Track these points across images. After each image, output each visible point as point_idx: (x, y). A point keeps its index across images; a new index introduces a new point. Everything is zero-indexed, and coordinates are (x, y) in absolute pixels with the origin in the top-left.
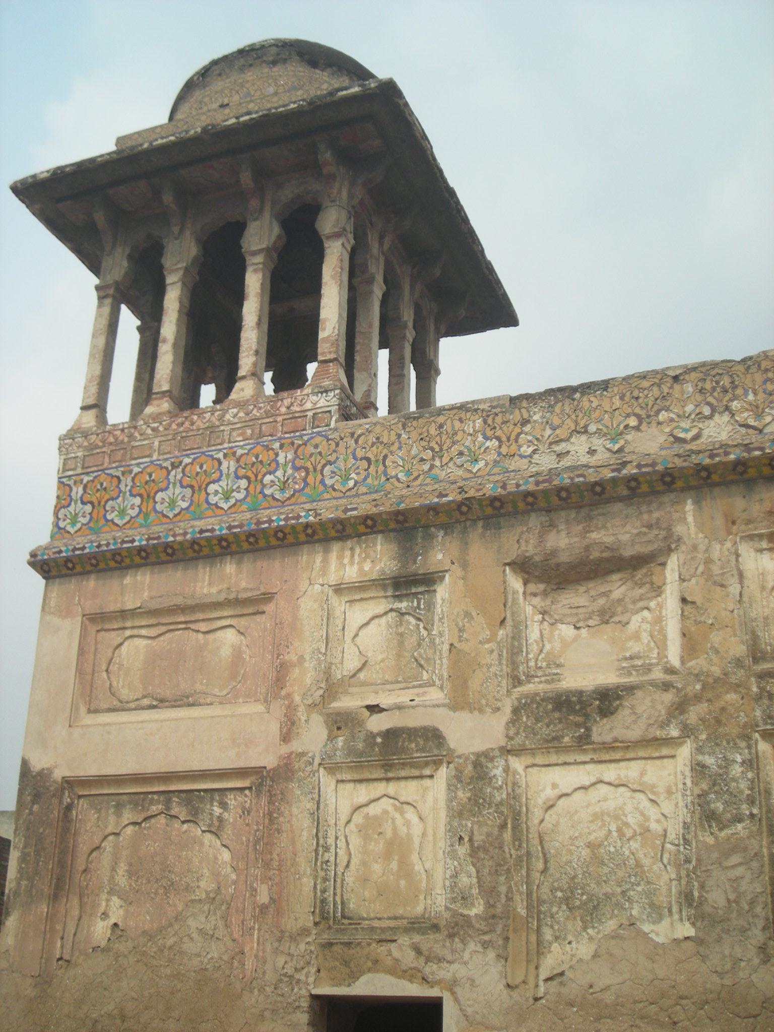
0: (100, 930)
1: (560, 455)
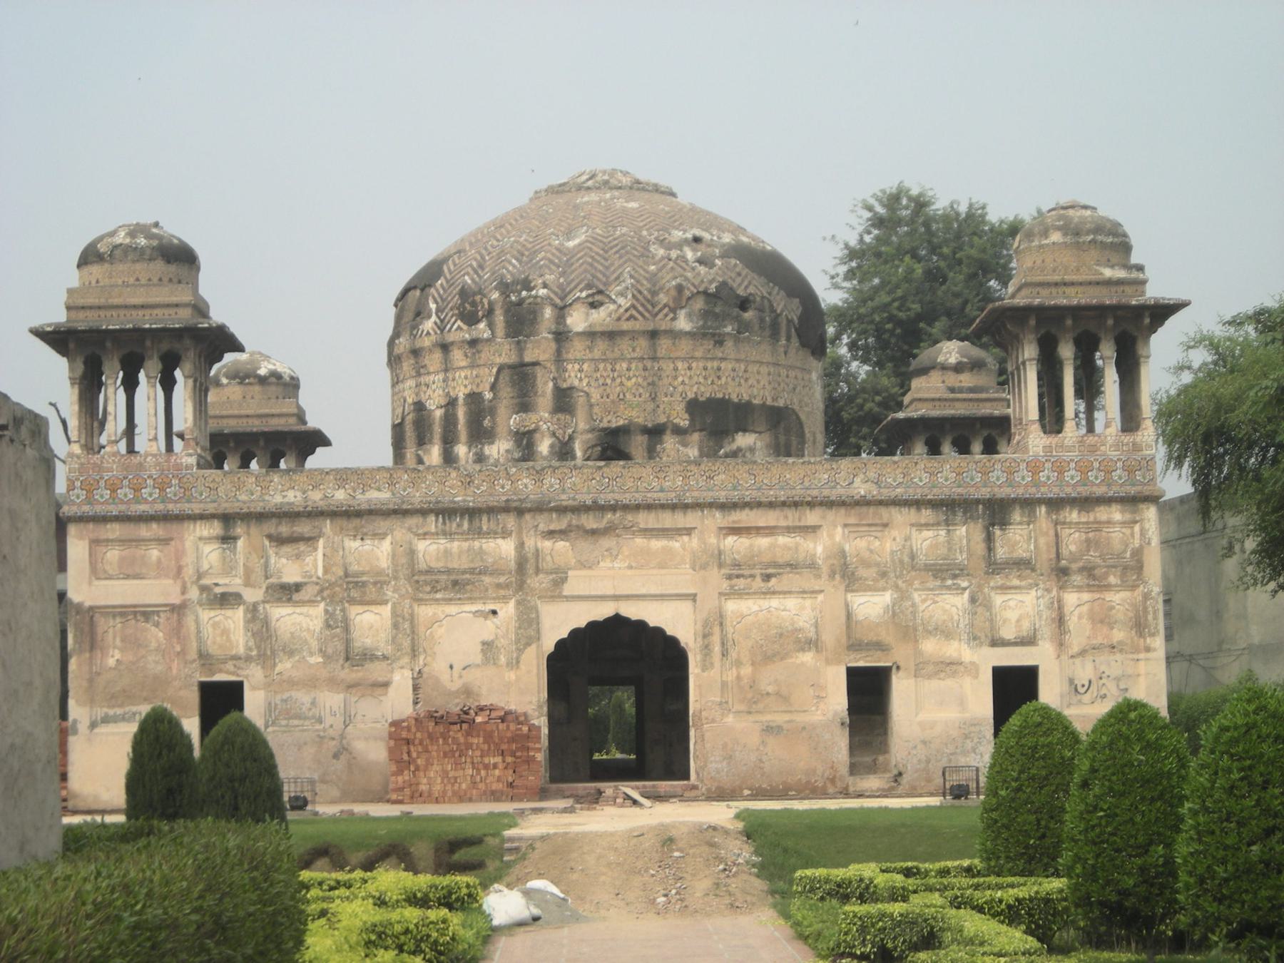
0: (111, 662)
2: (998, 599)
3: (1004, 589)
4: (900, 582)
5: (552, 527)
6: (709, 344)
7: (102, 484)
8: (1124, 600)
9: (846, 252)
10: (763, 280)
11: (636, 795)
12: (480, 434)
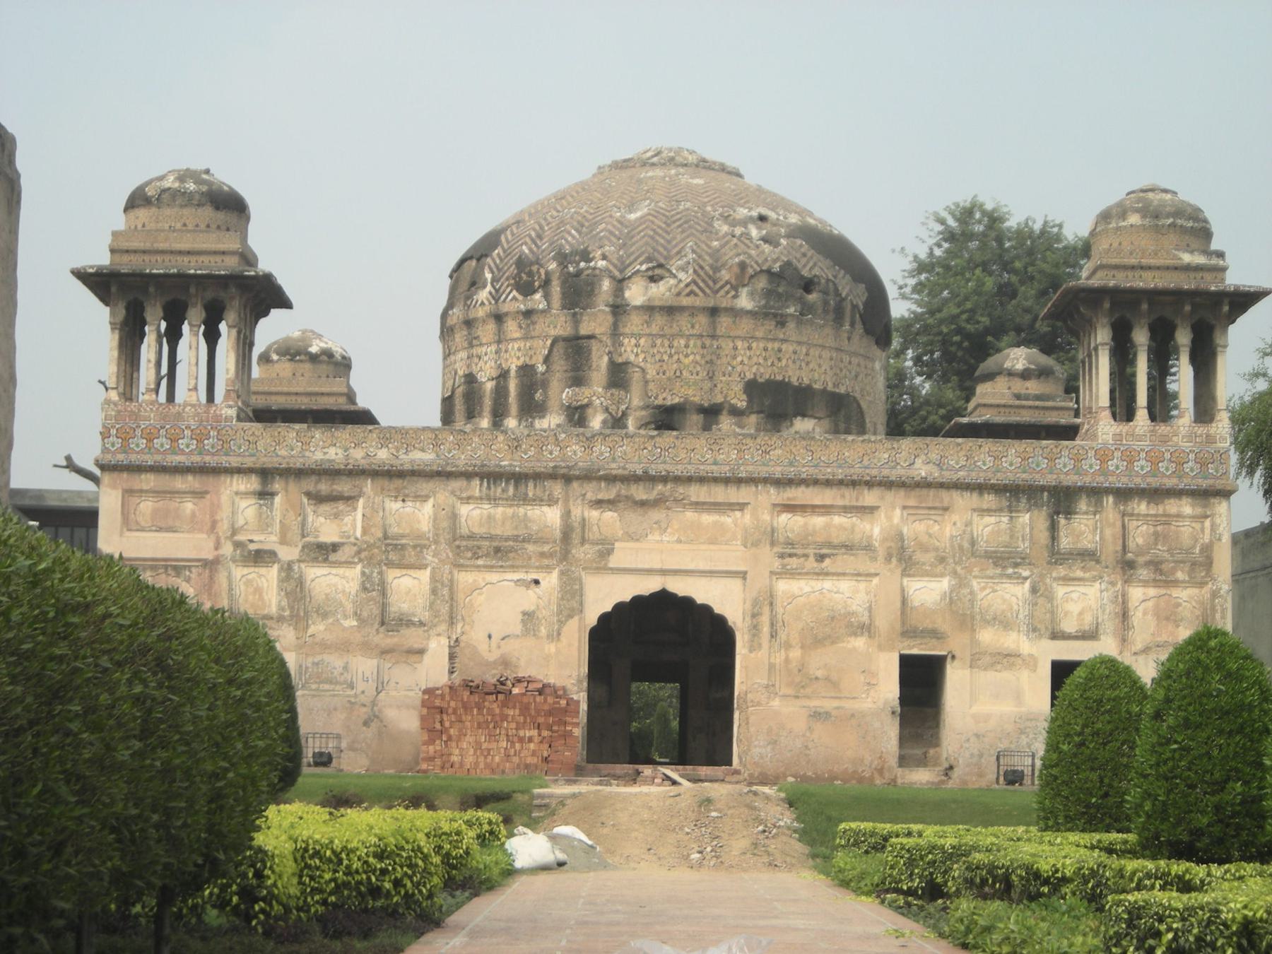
1: (325, 453)
2: (1060, 591)
3: (1067, 580)
4: (959, 569)
5: (600, 497)
6: (770, 325)
7: (139, 432)
8: (1191, 597)
9: (915, 265)
10: (829, 263)
11: (675, 776)
12: (531, 407)
